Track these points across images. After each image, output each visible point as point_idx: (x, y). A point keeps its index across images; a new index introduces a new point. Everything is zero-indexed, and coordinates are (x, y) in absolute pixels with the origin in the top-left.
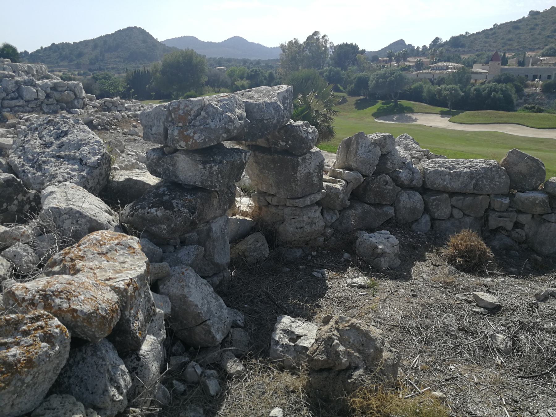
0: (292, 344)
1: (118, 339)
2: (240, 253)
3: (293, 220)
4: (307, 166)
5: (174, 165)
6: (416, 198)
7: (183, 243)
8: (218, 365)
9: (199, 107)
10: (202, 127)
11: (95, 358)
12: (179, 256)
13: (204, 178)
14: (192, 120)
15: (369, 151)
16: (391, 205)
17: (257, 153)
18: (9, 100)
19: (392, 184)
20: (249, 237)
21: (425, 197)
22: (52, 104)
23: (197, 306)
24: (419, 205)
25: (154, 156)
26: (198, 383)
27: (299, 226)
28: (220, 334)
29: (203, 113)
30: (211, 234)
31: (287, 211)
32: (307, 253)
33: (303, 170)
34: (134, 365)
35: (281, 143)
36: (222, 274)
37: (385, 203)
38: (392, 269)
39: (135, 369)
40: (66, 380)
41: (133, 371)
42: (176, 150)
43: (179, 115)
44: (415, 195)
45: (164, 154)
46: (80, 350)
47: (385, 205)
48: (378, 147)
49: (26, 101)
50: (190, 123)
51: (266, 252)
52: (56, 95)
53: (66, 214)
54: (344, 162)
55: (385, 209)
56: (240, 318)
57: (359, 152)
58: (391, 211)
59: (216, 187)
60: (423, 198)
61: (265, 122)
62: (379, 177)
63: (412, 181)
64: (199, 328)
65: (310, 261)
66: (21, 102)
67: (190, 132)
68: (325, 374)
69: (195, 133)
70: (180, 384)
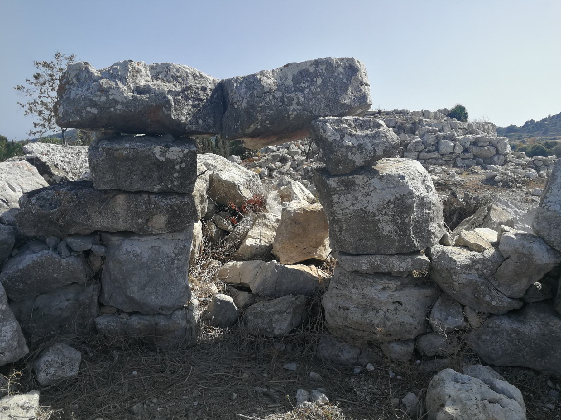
18: (426, 152)
22: (468, 159)
27: (342, 304)
49: (441, 155)
52: (475, 150)
57: (551, 198)
66: (436, 155)
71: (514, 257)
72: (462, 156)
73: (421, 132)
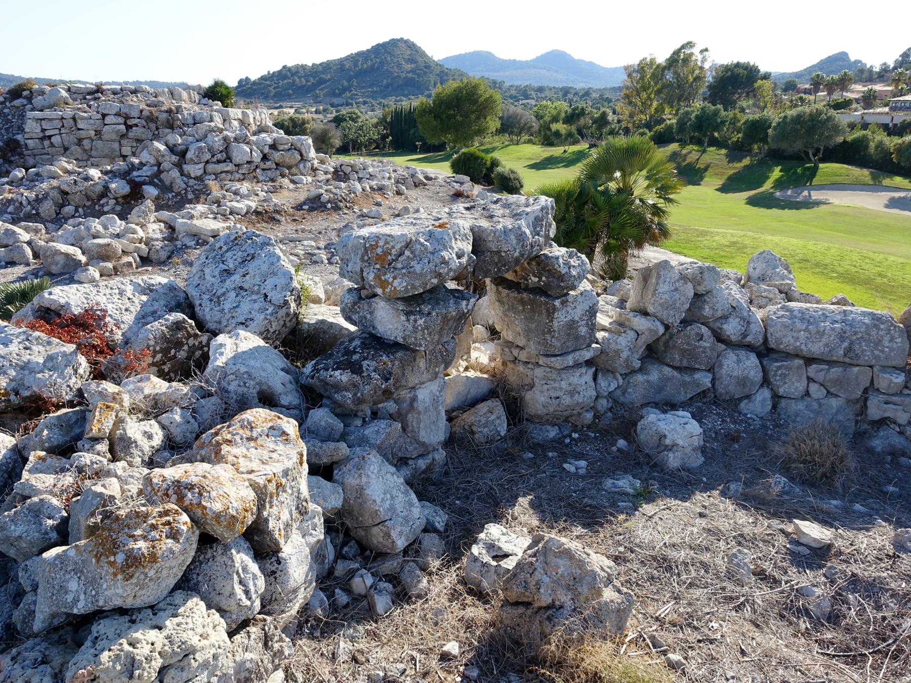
0: (494, 563)
1: (256, 538)
2: (466, 427)
3: (546, 387)
4: (570, 311)
5: (371, 313)
6: (748, 363)
7: (375, 415)
8: (395, 578)
9: (403, 244)
10: (404, 271)
11: (225, 558)
12: (366, 432)
13: (407, 333)
14: (393, 260)
15: (676, 290)
16: (709, 371)
17: (500, 288)
19: (712, 339)
20: (482, 404)
21: (765, 362)
22: (270, 169)
23: (374, 501)
24: (752, 373)
25: (349, 299)
26: (365, 596)
27: (554, 395)
28: (403, 538)
29: (407, 253)
30: (415, 405)
31: (539, 372)
32: (565, 433)
33: (562, 317)
34: (273, 569)
35: (533, 278)
36: (430, 456)
37: (697, 366)
38: (684, 470)
39: (274, 572)
40: (195, 576)
41: (271, 575)
42: (375, 295)
43: (377, 254)
44: (748, 359)
45: (360, 298)
46: (211, 548)
47: (698, 369)
48: (689, 283)
49: (236, 165)
50: (390, 264)
51: (503, 429)
52: (276, 156)
53: (233, 374)
54: (639, 302)
55: (697, 376)
56: (441, 520)
57: (660, 290)
58: (705, 380)
59: (421, 345)
60: (761, 363)
61: (503, 254)
62: (689, 328)
63: (745, 335)
64: (376, 528)
65: (567, 446)
66: (229, 167)
67: (389, 277)
68: (521, 610)
69: (395, 278)
70: (343, 594)
71: (647, 333)
72: (262, 166)
73: (199, 132)
